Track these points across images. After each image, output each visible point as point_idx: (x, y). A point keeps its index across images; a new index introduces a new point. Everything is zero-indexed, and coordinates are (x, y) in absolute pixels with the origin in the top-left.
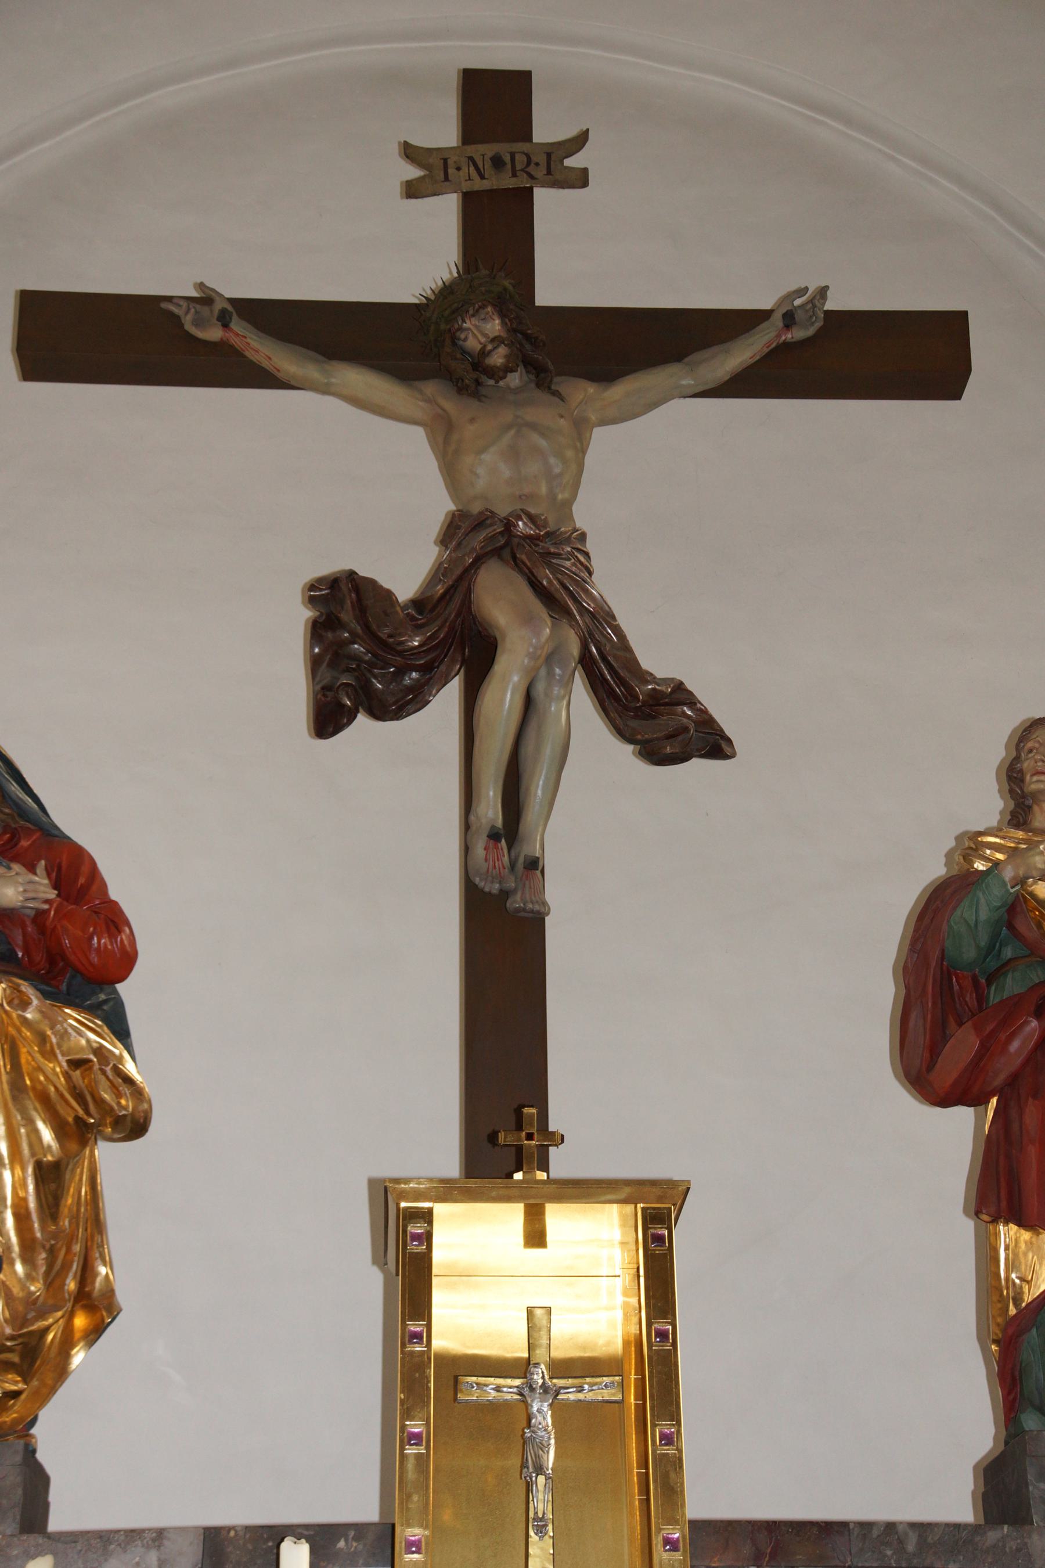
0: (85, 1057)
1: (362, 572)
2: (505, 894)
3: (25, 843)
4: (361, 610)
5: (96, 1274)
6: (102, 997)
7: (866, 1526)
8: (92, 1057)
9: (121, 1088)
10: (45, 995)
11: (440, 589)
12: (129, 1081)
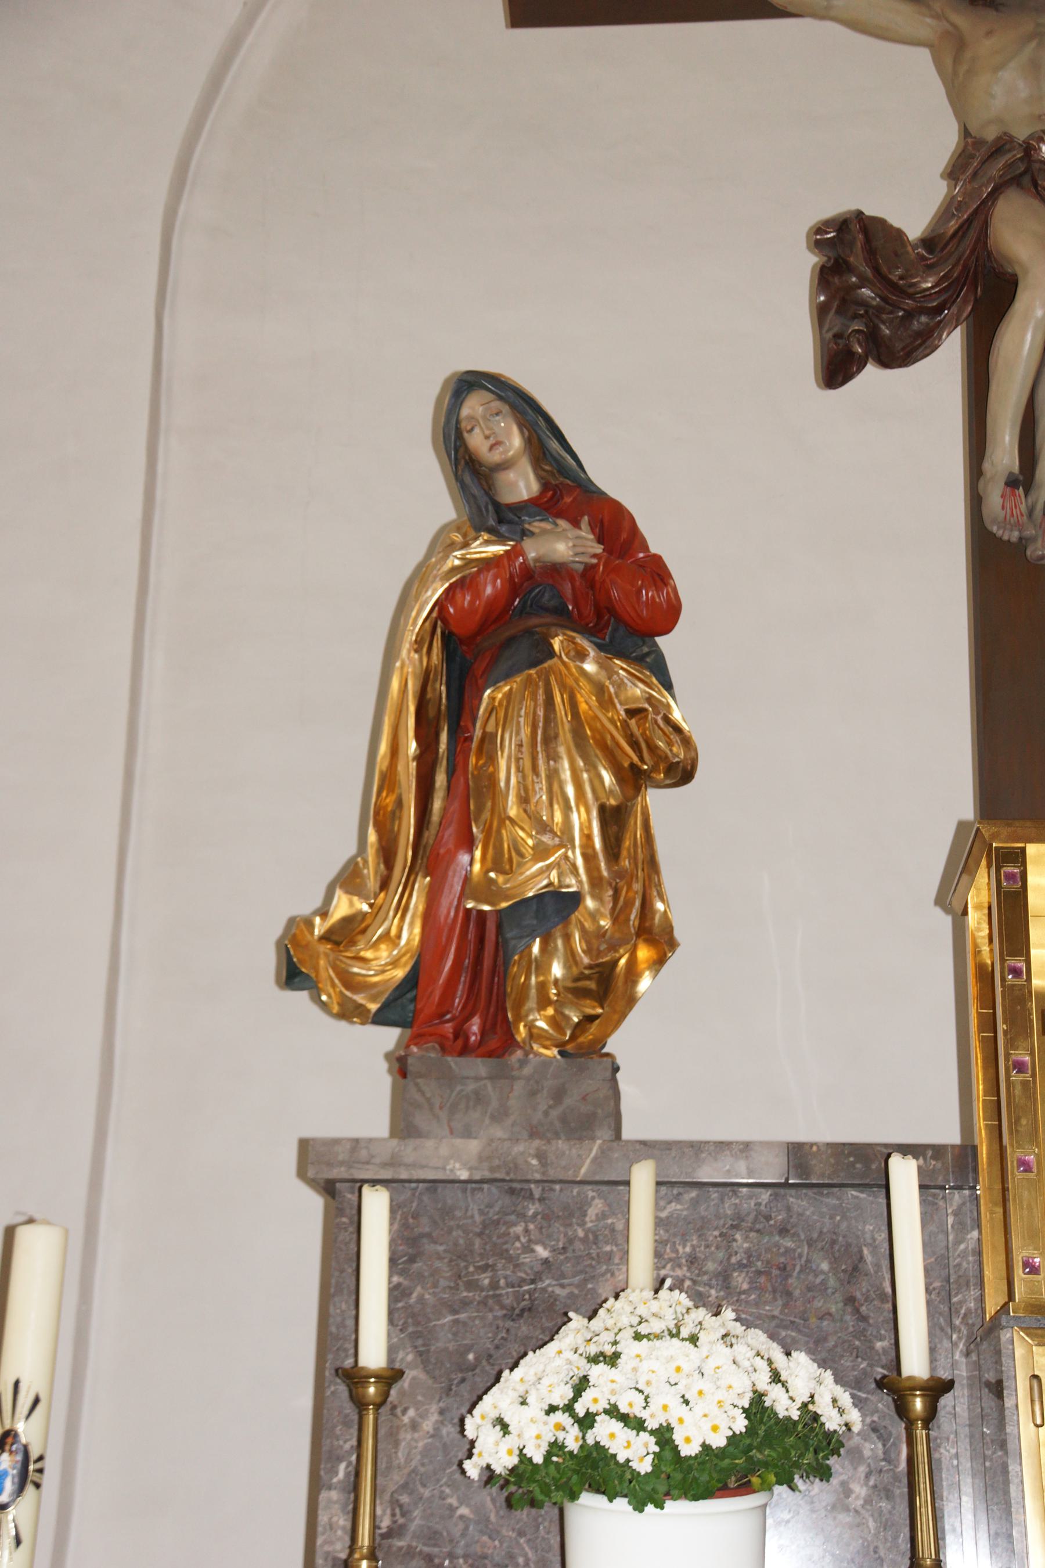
0: (641, 706)
1: (868, 212)
2: (1023, 543)
3: (568, 500)
4: (871, 252)
5: (654, 911)
6: (646, 649)
8: (647, 706)
9: (672, 737)
10: (600, 647)
11: (953, 225)
12: (678, 729)
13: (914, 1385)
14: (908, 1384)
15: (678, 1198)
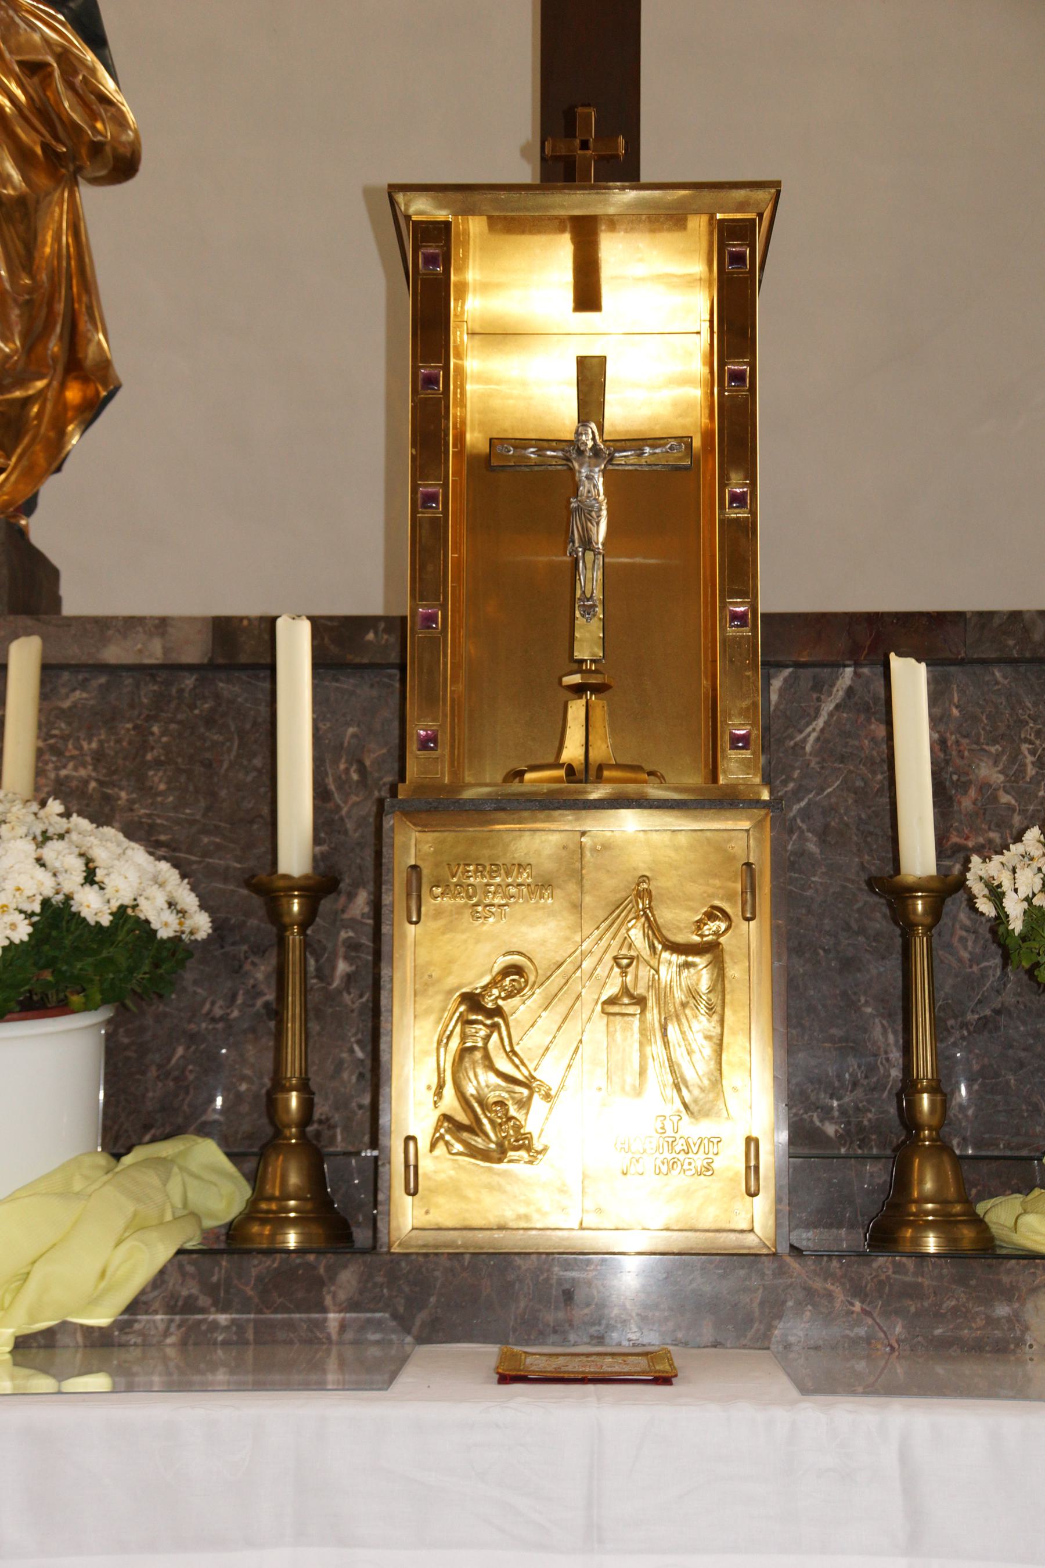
0: (40, 57)
7: (988, 616)
8: (50, 59)
9: (94, 107)
13: (291, 885)
14: (281, 883)
15: (83, 685)
